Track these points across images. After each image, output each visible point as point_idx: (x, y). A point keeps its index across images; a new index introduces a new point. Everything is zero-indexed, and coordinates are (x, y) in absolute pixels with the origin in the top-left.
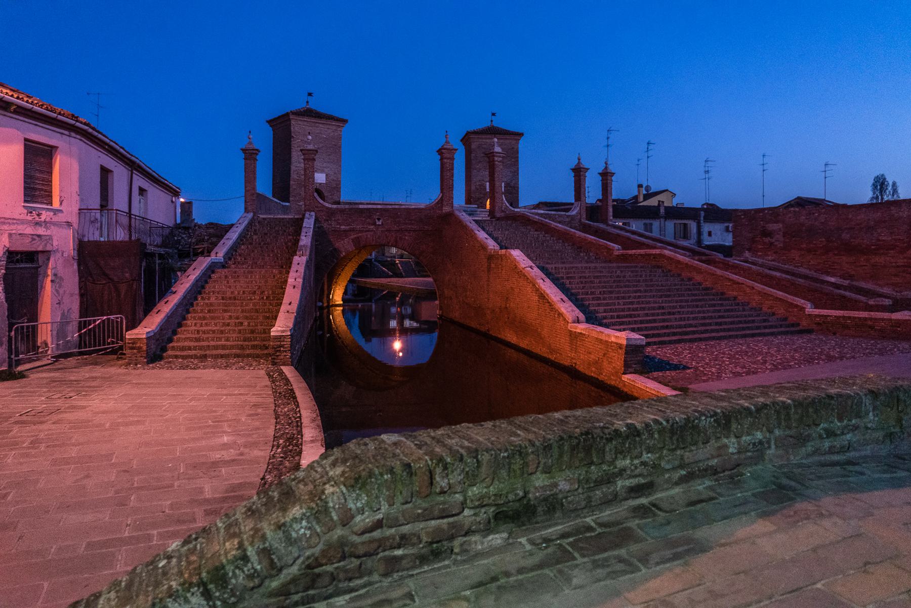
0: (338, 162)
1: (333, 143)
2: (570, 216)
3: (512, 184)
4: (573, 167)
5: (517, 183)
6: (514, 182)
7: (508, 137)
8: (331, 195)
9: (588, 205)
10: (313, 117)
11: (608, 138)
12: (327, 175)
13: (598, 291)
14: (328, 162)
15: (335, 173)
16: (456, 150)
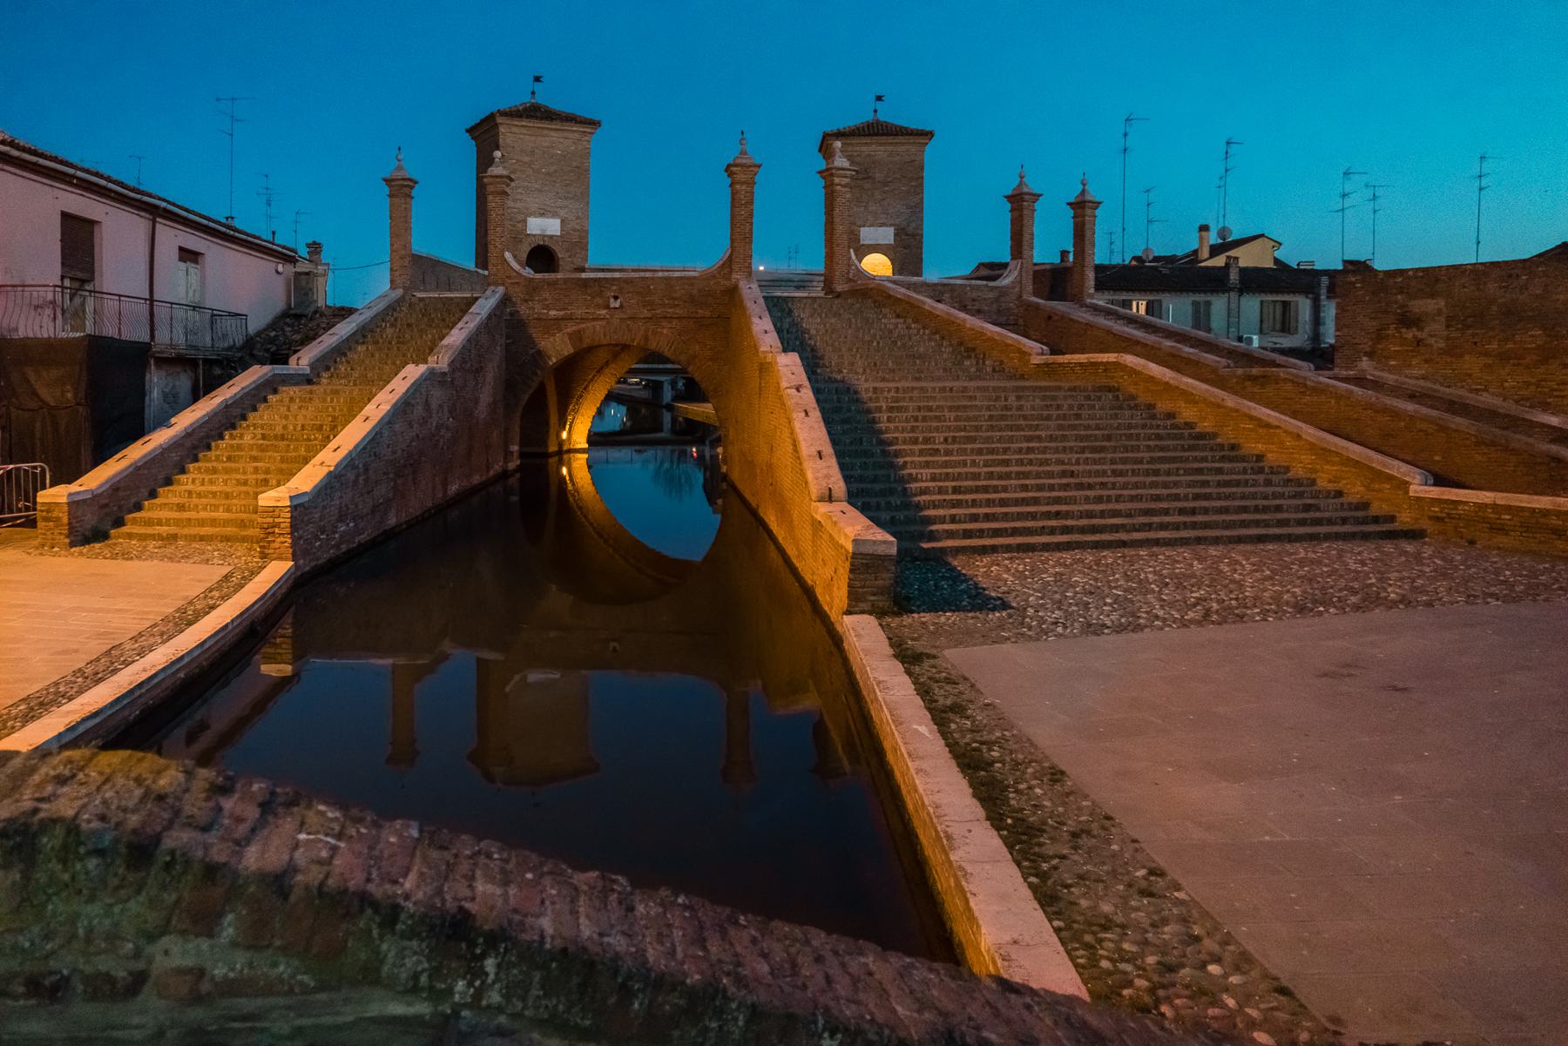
0: (584, 197)
1: (575, 164)
2: (997, 288)
3: (910, 230)
4: (1009, 193)
5: (920, 227)
6: (913, 225)
7: (901, 139)
8: (570, 257)
9: (1037, 268)
10: (537, 118)
11: (1125, 135)
12: (562, 221)
13: (940, 437)
14: (566, 198)
15: (578, 218)
16: (759, 166)
